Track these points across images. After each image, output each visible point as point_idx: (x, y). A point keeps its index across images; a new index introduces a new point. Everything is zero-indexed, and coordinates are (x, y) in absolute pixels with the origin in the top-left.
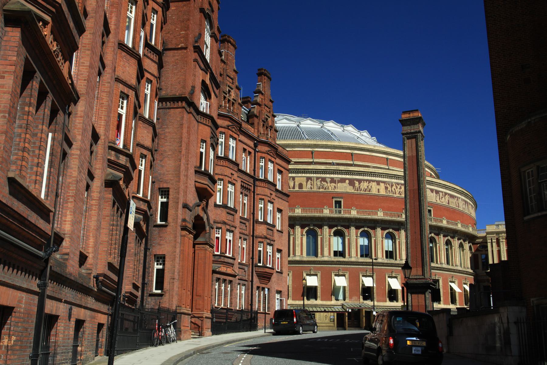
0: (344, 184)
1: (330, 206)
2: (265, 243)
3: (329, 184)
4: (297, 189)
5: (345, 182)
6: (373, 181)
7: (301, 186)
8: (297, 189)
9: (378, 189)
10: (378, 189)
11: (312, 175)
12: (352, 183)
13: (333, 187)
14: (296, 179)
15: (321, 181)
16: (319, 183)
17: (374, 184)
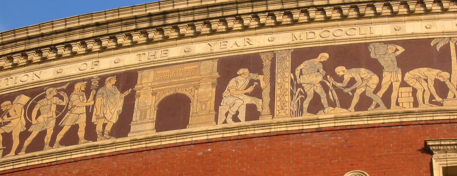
3: (391, 76)
7: (174, 111)
11: (259, 41)
14: (145, 81)
15: (329, 68)
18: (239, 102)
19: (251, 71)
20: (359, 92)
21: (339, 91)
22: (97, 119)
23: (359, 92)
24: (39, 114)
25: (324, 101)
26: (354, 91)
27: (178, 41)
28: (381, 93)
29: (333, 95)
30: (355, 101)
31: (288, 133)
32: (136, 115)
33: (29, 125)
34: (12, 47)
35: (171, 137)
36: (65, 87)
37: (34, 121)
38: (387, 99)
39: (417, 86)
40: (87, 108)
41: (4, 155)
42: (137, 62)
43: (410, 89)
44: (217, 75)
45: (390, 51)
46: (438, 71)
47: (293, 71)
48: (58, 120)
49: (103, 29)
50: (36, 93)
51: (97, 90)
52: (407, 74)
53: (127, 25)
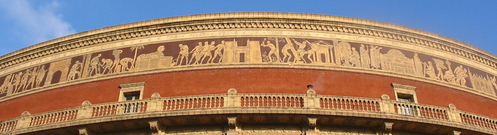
0: (153, 56)
9: (242, 55)
10: (242, 55)
14: (52, 66)
18: (74, 73)
19: (80, 62)
20: (106, 68)
21: (101, 67)
22: (37, 80)
23: (106, 68)
24: (23, 79)
25: (96, 71)
26: (105, 67)
27: (63, 52)
28: (112, 68)
29: (99, 69)
30: (104, 71)
31: (84, 83)
32: (47, 78)
33: (20, 82)
34: (19, 56)
36: (31, 69)
37: (22, 81)
38: (113, 70)
39: (123, 64)
40: (36, 76)
41: (12, 94)
42: (51, 60)
43: (120, 66)
44: (70, 63)
45: (118, 52)
46: (130, 58)
47: (90, 62)
48: (28, 81)
49: (42, 49)
50: (24, 71)
51: (39, 70)
52: (121, 60)
53: (49, 47)
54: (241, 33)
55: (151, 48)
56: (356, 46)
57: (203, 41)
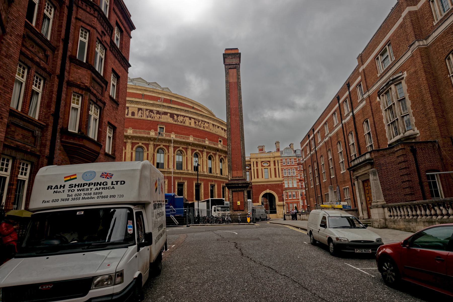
1: (156, 130)
2: (87, 98)
3: (155, 115)
4: (130, 116)
5: (167, 115)
6: (187, 117)
7: (133, 114)
8: (130, 116)
12: (172, 116)
13: (158, 117)
14: (130, 108)
15: (149, 112)
16: (147, 113)
17: (187, 119)
35: (133, 117)
54: (190, 116)
55: (166, 113)
56: (213, 125)
57: (181, 115)
